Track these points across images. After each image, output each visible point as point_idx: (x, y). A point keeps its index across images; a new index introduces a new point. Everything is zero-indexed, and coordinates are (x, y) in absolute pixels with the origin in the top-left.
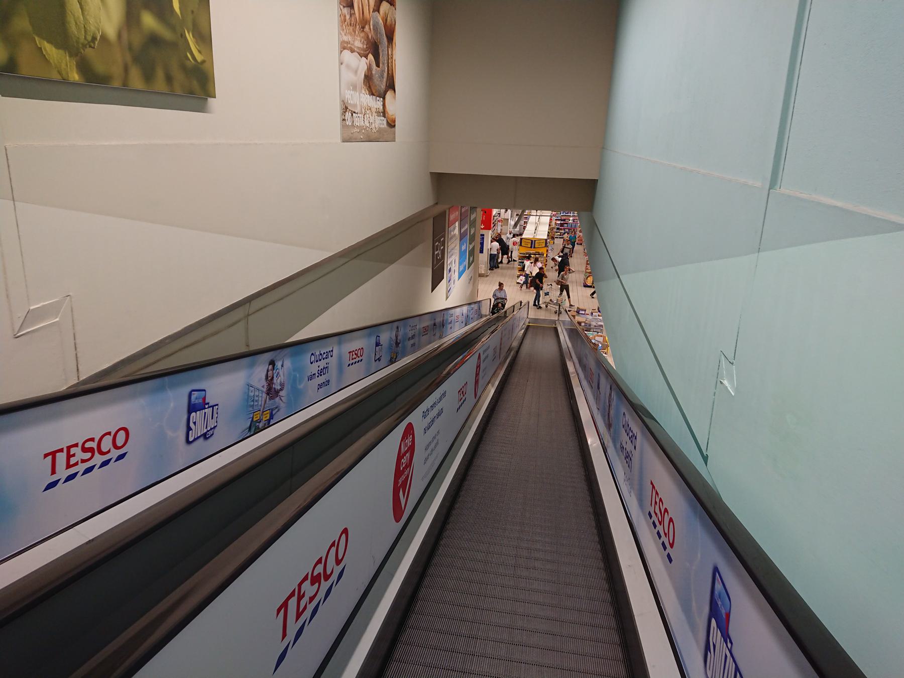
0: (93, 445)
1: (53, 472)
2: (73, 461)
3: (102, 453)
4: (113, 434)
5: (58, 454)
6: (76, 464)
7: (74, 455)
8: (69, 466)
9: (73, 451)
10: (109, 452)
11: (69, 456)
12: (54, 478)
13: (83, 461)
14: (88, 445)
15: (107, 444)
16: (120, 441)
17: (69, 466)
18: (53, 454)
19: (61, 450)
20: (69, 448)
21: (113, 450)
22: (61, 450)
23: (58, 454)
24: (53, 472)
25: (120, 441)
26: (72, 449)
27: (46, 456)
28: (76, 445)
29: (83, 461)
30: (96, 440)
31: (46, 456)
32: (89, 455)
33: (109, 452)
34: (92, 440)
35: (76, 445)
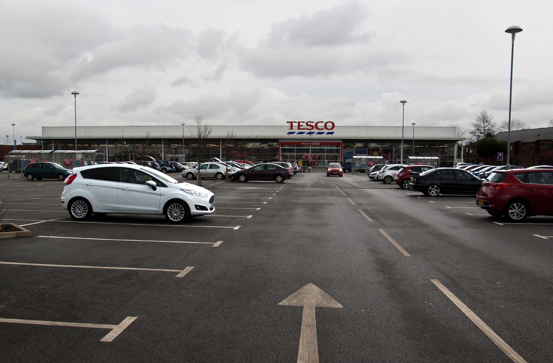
0: (314, 125)
1: (292, 128)
2: (301, 127)
3: (317, 128)
4: (324, 123)
5: (294, 124)
6: (304, 129)
7: (302, 126)
10: (323, 129)
13: (307, 129)
14: (309, 123)
16: (330, 125)
17: (299, 128)
18: (292, 123)
19: (296, 122)
20: (299, 123)
21: (324, 128)
22: (296, 122)
23: (293, 123)
24: (292, 128)
25: (330, 125)
26: (300, 123)
27: (287, 122)
28: (304, 122)
29: (307, 129)
31: (287, 122)
33: (323, 129)
34: (313, 122)
35: (304, 122)
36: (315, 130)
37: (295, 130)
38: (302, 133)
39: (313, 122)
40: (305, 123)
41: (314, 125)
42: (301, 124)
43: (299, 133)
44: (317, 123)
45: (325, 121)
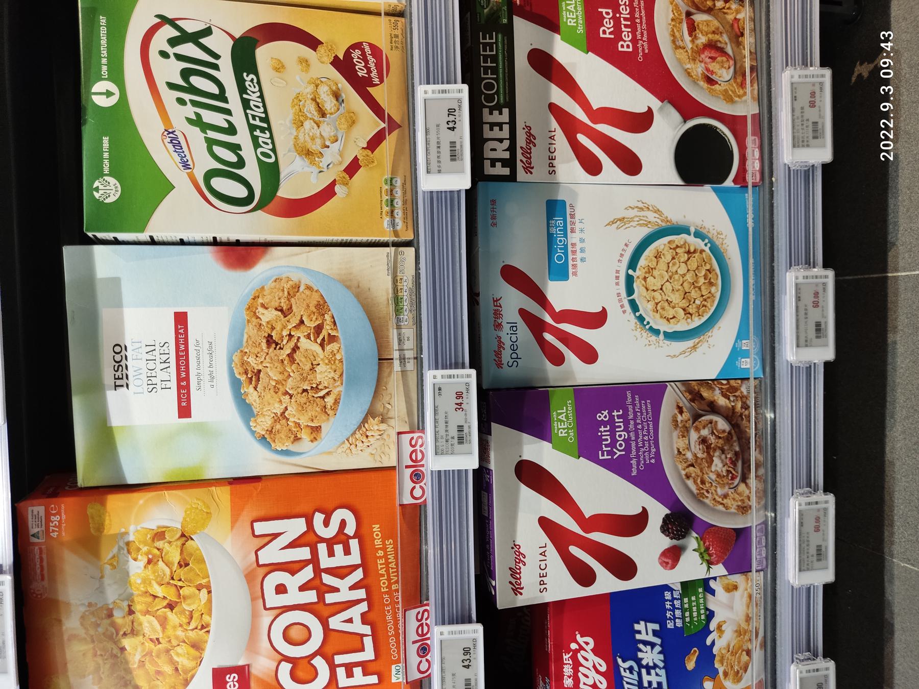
0: (117, 365)
2: (121, 377)
8: (122, 379)
9: (117, 377)
10: (122, 356)
11: (119, 378)
12: (125, 385)
13: (122, 371)
14: (116, 369)
15: (118, 358)
16: (117, 349)
17: (122, 379)
18: (116, 386)
19: (115, 382)
20: (115, 379)
21: (121, 354)
22: (115, 382)
28: (115, 375)
29: (122, 371)
30: (115, 364)
32: (120, 368)
33: (122, 356)
34: (114, 366)
35: (115, 375)
36: (123, 363)
37: (123, 382)
38: (127, 376)
39: (114, 366)
40: (115, 373)
41: (117, 365)
42: (117, 377)
43: (127, 378)
44: (116, 362)
45: (115, 354)
